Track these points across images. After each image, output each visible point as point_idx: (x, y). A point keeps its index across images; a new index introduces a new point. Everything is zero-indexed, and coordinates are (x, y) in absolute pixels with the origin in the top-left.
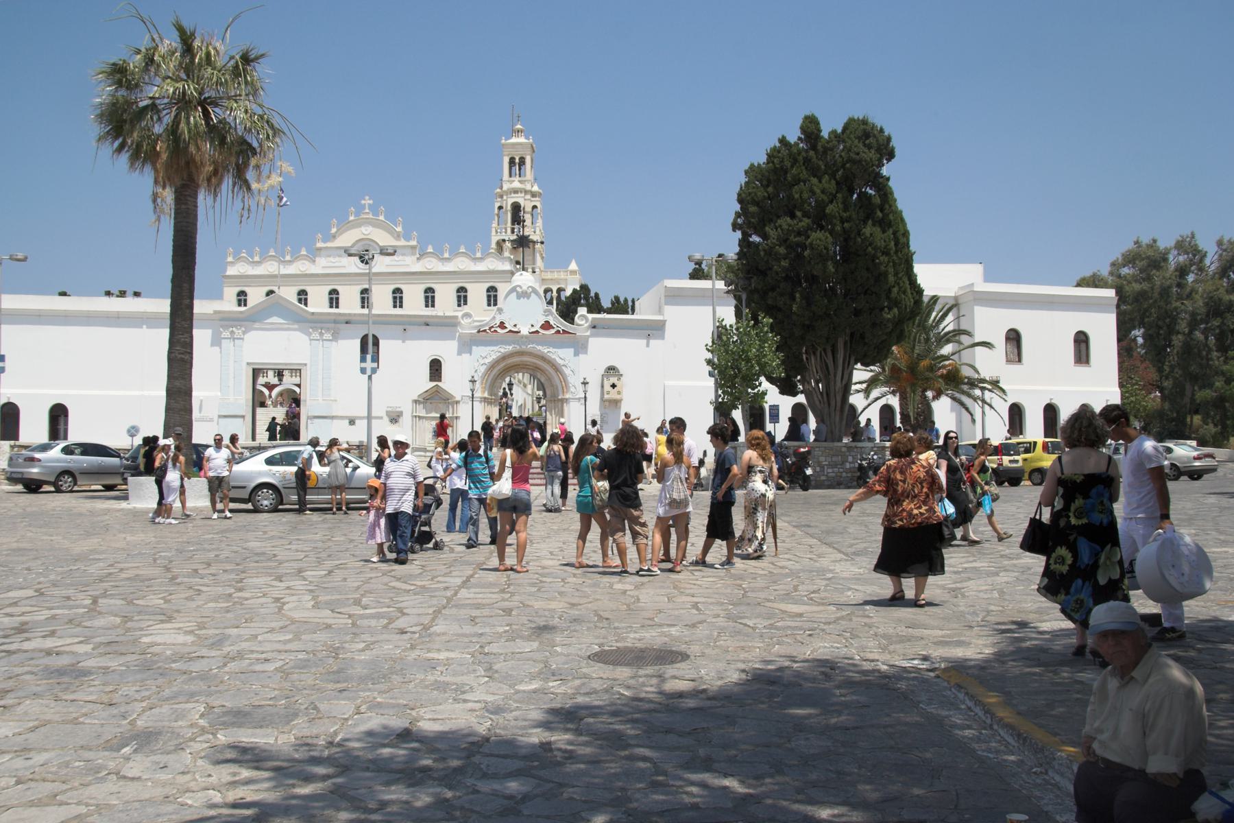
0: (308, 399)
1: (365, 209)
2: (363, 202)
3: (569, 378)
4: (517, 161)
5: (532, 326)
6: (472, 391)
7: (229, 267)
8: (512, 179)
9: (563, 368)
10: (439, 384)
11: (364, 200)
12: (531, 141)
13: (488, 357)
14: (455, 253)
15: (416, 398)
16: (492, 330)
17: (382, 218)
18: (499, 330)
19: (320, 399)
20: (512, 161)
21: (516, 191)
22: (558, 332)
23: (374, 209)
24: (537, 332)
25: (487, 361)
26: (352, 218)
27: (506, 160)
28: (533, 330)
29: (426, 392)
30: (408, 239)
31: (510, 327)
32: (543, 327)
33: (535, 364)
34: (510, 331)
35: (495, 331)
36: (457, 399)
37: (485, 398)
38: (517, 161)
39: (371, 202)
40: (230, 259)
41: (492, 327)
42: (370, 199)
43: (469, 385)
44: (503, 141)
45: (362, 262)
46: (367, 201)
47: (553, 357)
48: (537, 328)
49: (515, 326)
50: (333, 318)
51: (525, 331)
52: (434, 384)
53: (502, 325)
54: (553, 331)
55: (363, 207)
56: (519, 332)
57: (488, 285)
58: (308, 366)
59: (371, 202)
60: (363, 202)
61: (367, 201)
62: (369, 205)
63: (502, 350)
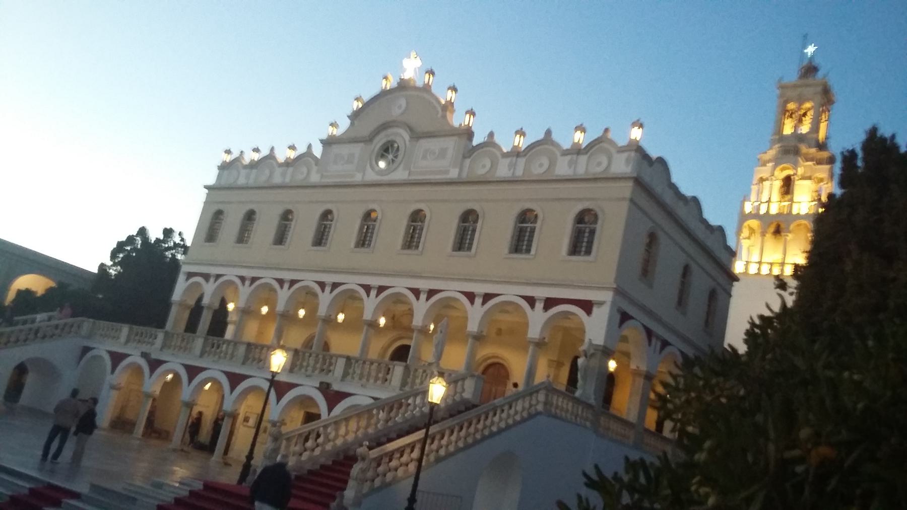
57: (580, 207)
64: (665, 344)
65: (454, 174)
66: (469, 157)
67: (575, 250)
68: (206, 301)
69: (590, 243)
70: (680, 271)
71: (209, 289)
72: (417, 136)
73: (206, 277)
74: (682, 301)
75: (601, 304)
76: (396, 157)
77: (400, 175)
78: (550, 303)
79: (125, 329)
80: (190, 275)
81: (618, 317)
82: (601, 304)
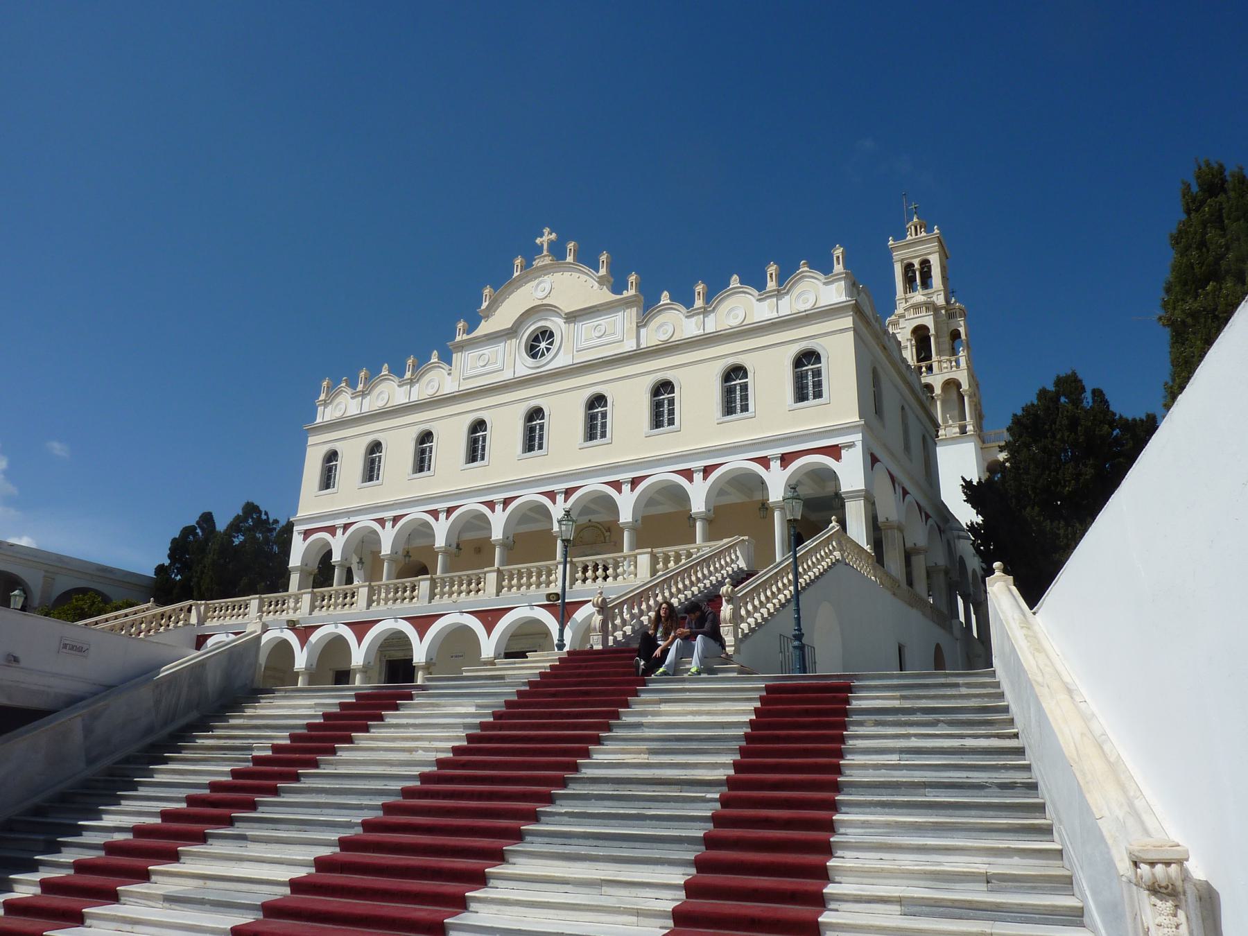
4: (917, 266)
7: (320, 409)
11: (542, 235)
12: (936, 231)
14: (716, 289)
20: (908, 268)
21: (916, 307)
23: (558, 251)
30: (618, 287)
38: (917, 266)
39: (553, 236)
40: (322, 397)
42: (550, 233)
44: (891, 242)
45: (534, 356)
46: (546, 237)
55: (539, 249)
57: (795, 349)
60: (538, 241)
62: (551, 243)
64: (905, 493)
65: (629, 345)
66: (644, 326)
67: (801, 396)
68: (336, 557)
69: (818, 385)
70: (900, 409)
71: (337, 545)
72: (572, 317)
73: (332, 530)
74: (907, 448)
75: (850, 445)
76: (551, 344)
77: (561, 358)
78: (786, 460)
79: (254, 602)
80: (307, 534)
81: (869, 458)
82: (850, 445)
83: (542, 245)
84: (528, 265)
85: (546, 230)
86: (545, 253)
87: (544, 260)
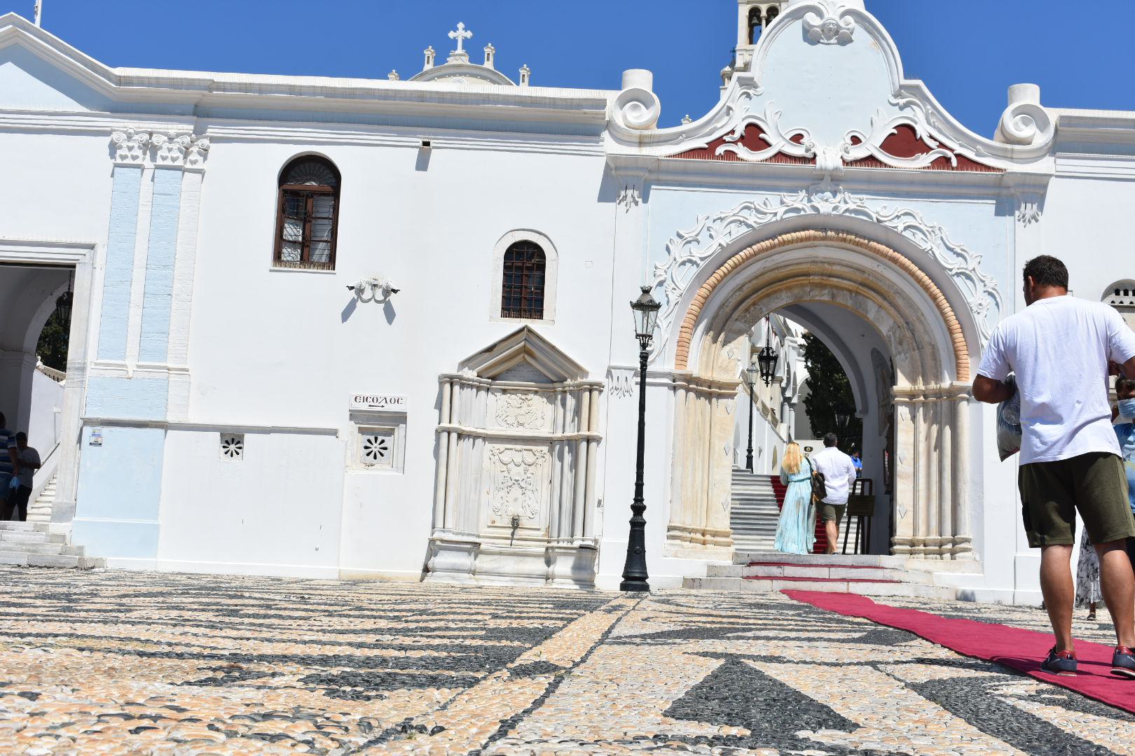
0: (92, 357)
1: (456, 49)
2: (451, 35)
3: (979, 319)
5: (856, 140)
6: (644, 339)
8: (752, 47)
9: (959, 281)
10: (534, 324)
11: (456, 29)
13: (703, 237)
15: (453, 371)
16: (720, 150)
17: (489, 65)
18: (741, 151)
19: (131, 363)
20: (754, 13)
22: (944, 162)
24: (871, 160)
25: (698, 252)
26: (428, 67)
27: (743, 12)
28: (859, 152)
29: (490, 349)
31: (778, 143)
32: (890, 145)
33: (861, 270)
34: (780, 156)
35: (730, 155)
36: (591, 378)
37: (689, 379)
38: (764, 13)
39: (469, 34)
41: (720, 141)
43: (633, 320)
46: (461, 33)
47: (925, 246)
48: (871, 146)
49: (797, 138)
50: (194, 95)
51: (829, 159)
52: (515, 324)
53: (753, 137)
54: (924, 160)
56: (813, 159)
58: (101, 251)
59: (469, 34)
60: (451, 35)
61: (461, 33)
62: (465, 40)
63: (752, 219)
83: (455, 40)
84: (440, 59)
85: (461, 25)
86: (460, 50)
87: (459, 57)
